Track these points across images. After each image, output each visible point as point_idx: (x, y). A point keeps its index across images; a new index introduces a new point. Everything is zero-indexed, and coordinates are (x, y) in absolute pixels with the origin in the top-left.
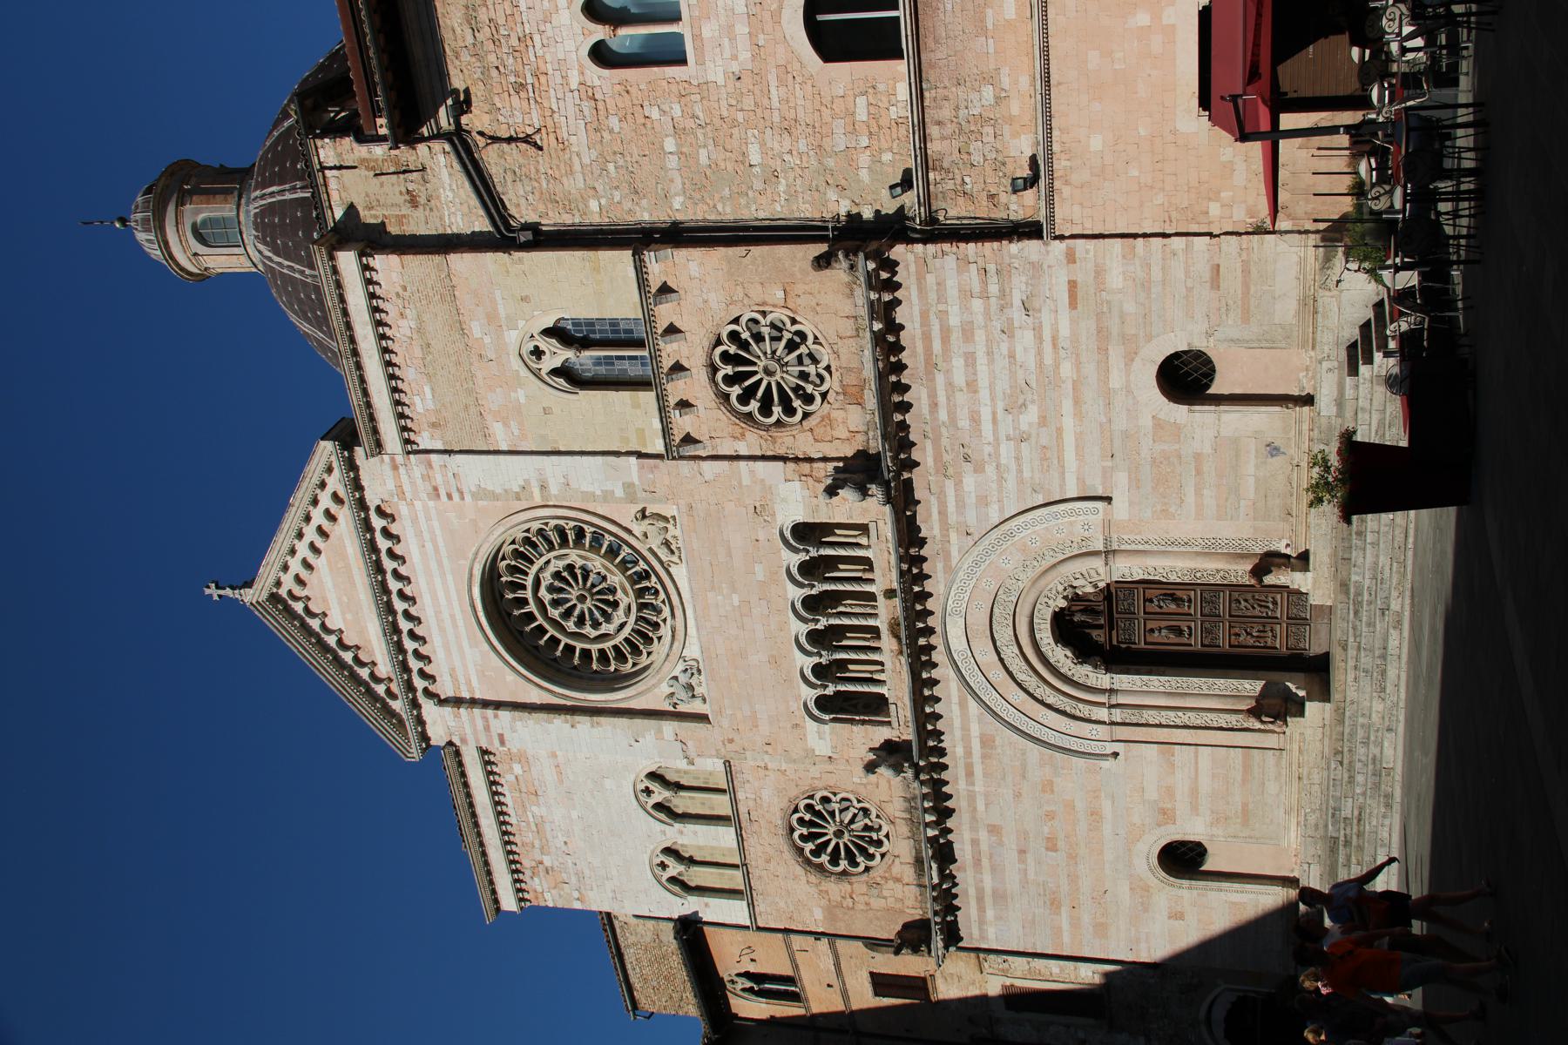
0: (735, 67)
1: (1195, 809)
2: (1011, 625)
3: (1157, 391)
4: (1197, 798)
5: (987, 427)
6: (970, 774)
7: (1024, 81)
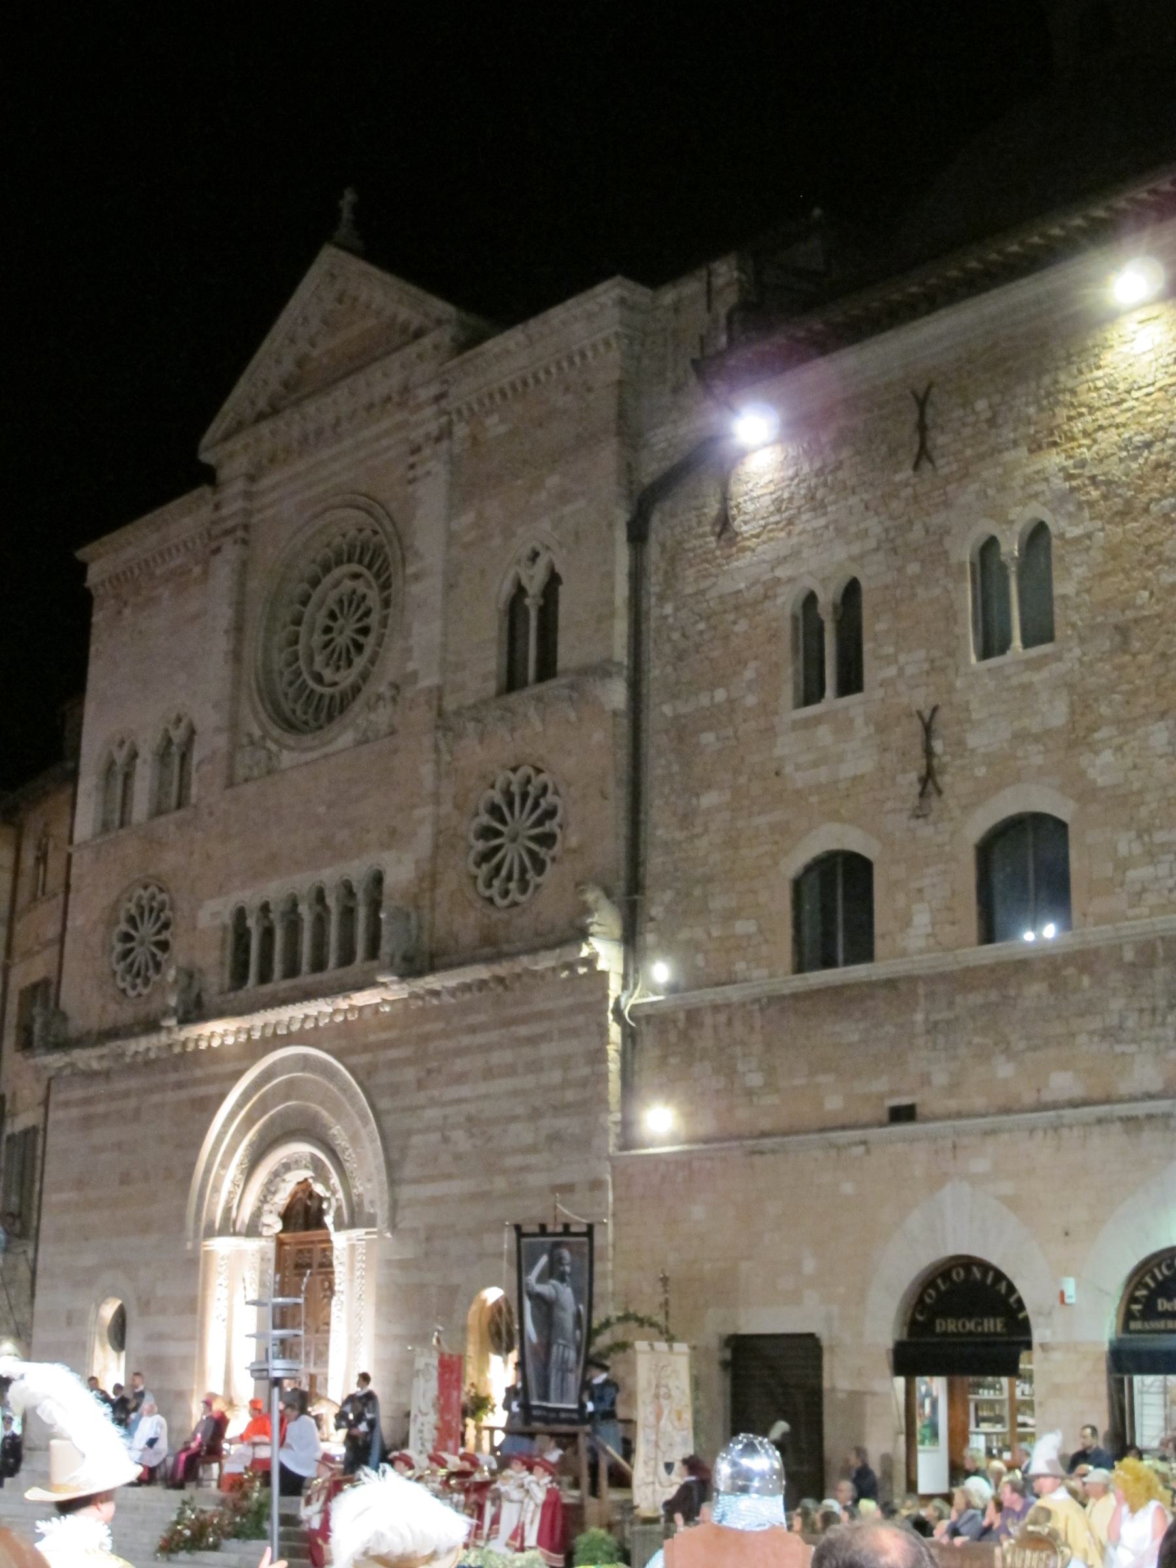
0: (788, 769)
6: (179, 1085)
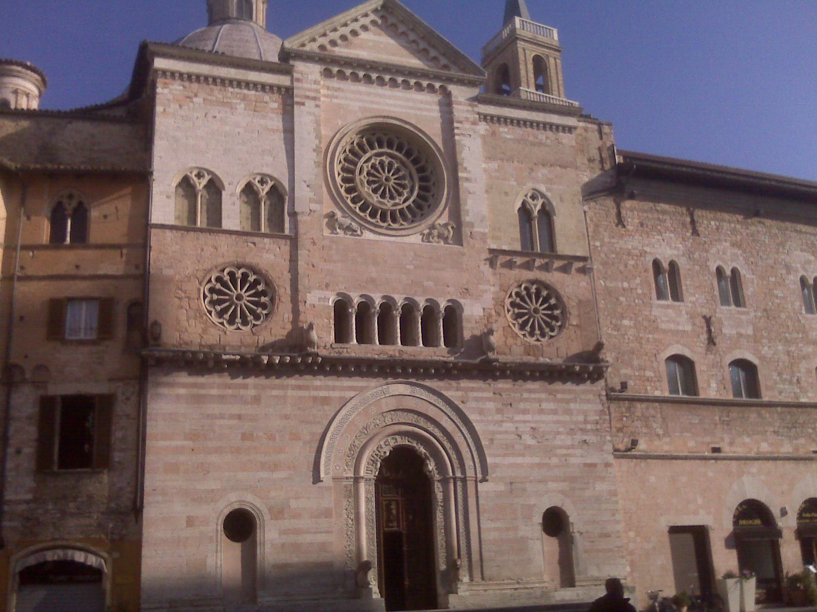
1: (285, 532)
3: (549, 507)
5: (519, 417)
6: (300, 388)
7: (666, 448)
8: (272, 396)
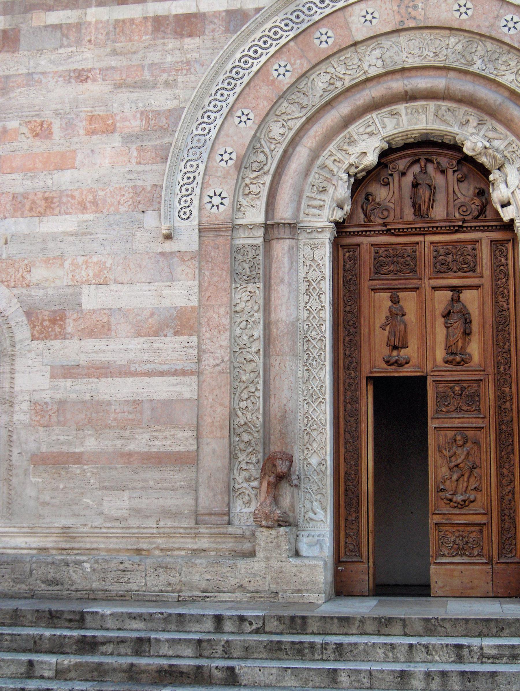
2: (425, 63)
4: (88, 376)
8: (46, 27)
